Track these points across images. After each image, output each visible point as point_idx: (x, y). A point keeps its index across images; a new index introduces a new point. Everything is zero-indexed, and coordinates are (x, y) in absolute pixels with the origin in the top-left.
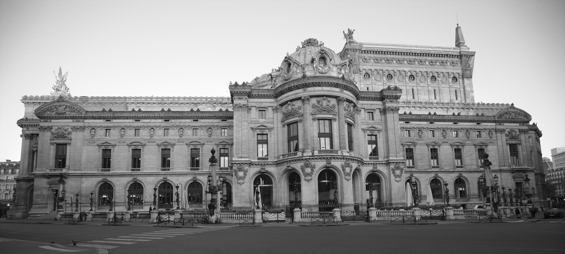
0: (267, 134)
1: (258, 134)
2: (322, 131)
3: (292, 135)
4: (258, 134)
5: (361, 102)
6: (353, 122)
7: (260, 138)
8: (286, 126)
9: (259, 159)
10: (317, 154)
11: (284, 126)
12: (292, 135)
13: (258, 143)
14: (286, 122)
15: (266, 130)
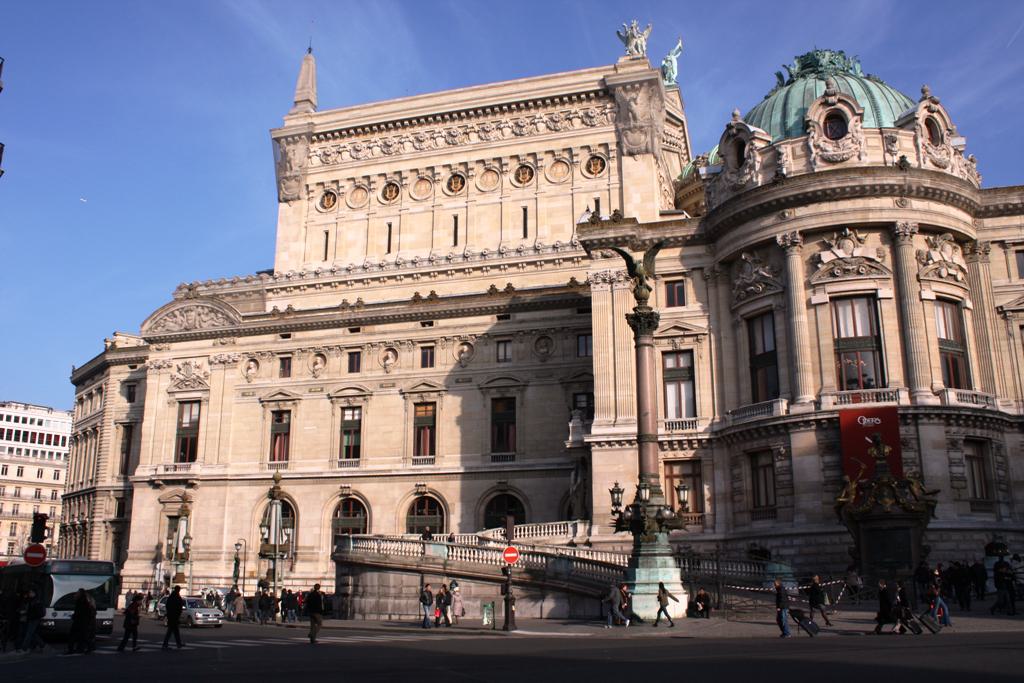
0: (691, 352)
1: (664, 353)
2: (848, 332)
3: (759, 351)
4: (664, 353)
5: (988, 222)
6: (959, 292)
7: (670, 363)
8: (744, 323)
9: (670, 426)
10: (832, 407)
11: (735, 326)
12: (759, 351)
13: (666, 381)
14: (743, 311)
15: (686, 340)
